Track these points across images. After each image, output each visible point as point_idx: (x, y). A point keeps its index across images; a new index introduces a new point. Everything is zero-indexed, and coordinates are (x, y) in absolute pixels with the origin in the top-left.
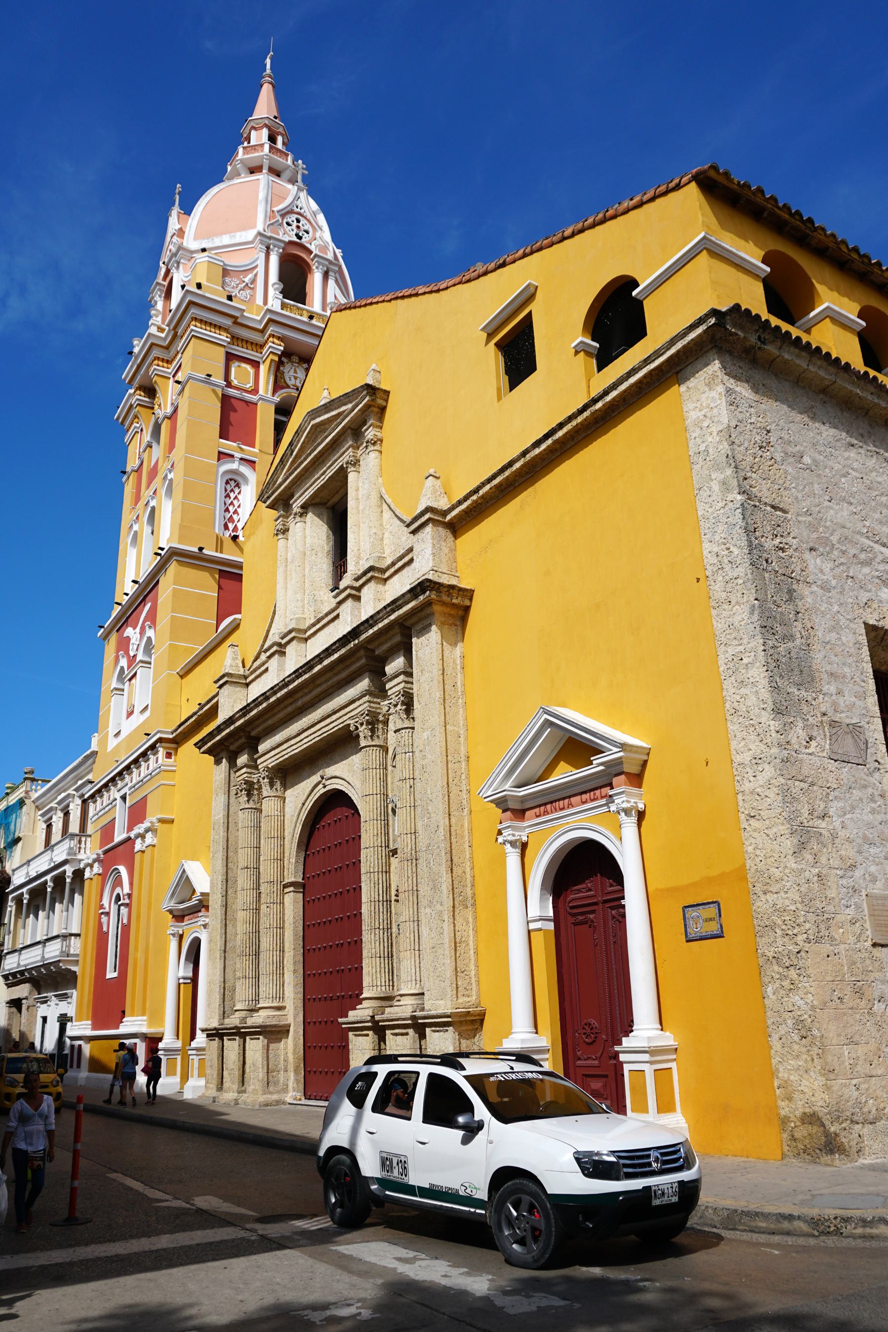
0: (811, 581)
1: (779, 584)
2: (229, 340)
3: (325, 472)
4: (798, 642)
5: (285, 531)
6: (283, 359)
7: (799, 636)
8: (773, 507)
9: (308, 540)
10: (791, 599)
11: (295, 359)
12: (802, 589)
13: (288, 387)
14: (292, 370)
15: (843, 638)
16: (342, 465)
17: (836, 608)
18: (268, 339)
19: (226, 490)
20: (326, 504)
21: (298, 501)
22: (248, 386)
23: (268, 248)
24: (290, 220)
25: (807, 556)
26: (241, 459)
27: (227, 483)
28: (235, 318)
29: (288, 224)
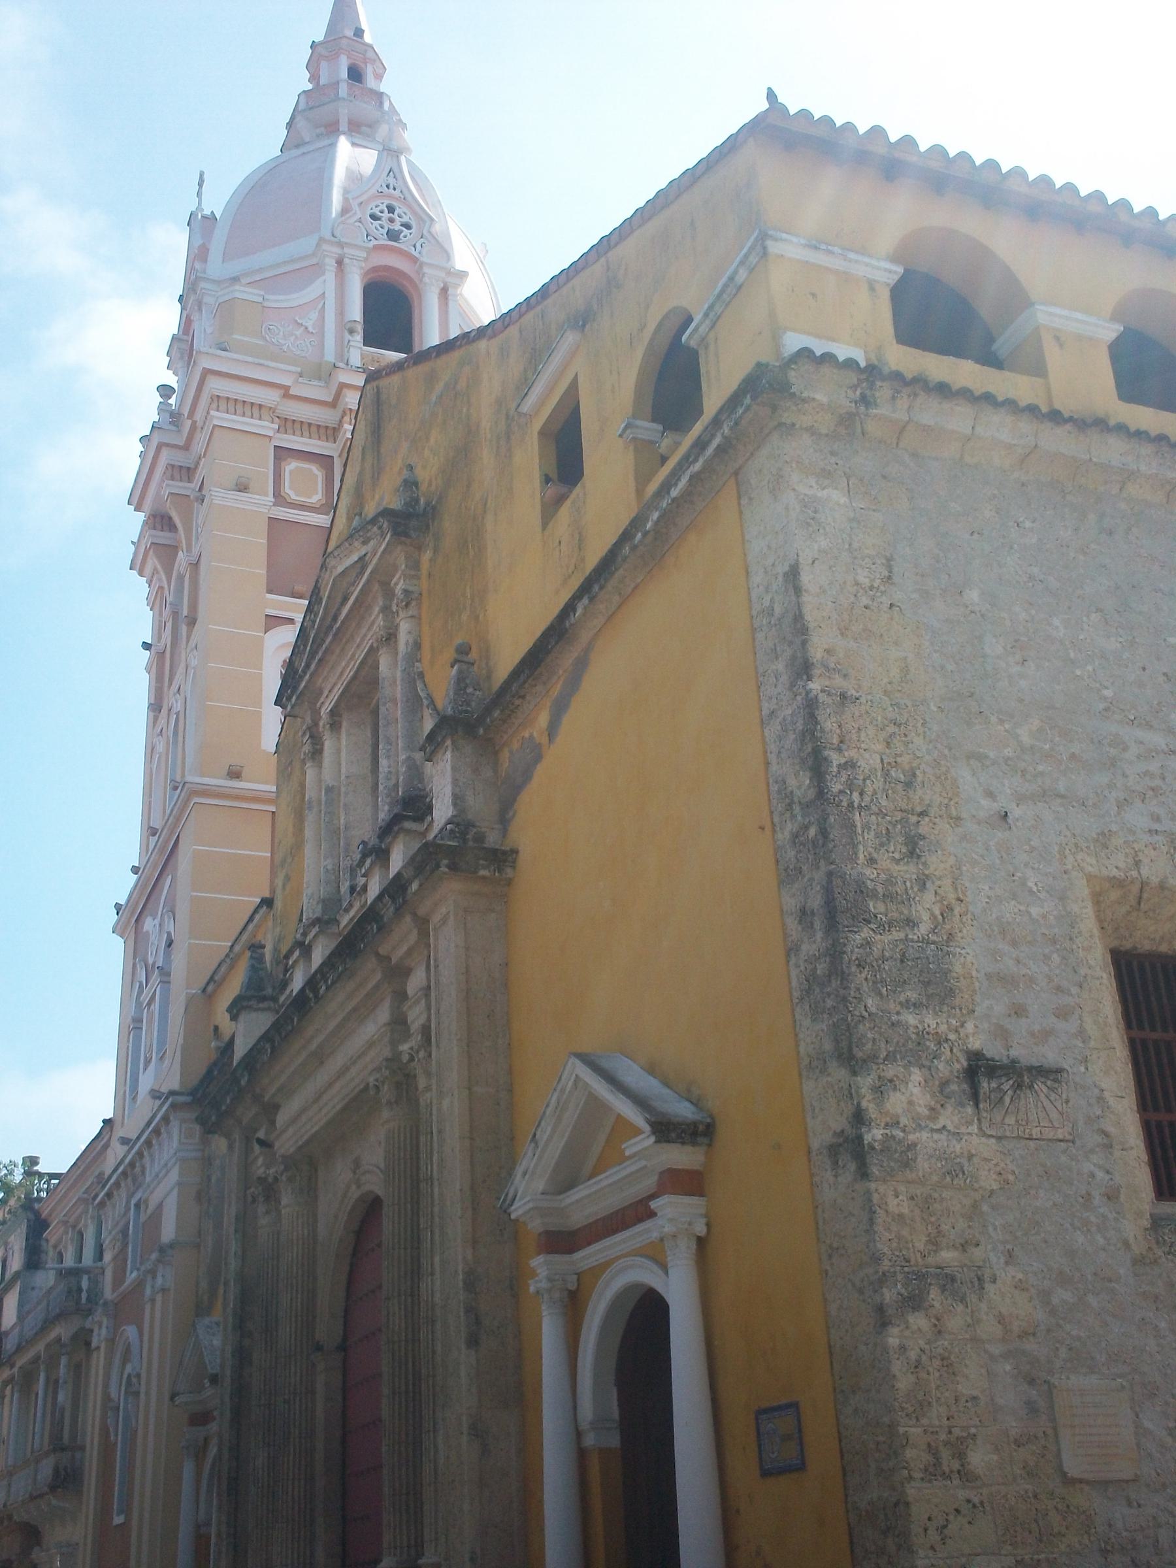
3: (353, 655)
16: (372, 646)
21: (327, 704)
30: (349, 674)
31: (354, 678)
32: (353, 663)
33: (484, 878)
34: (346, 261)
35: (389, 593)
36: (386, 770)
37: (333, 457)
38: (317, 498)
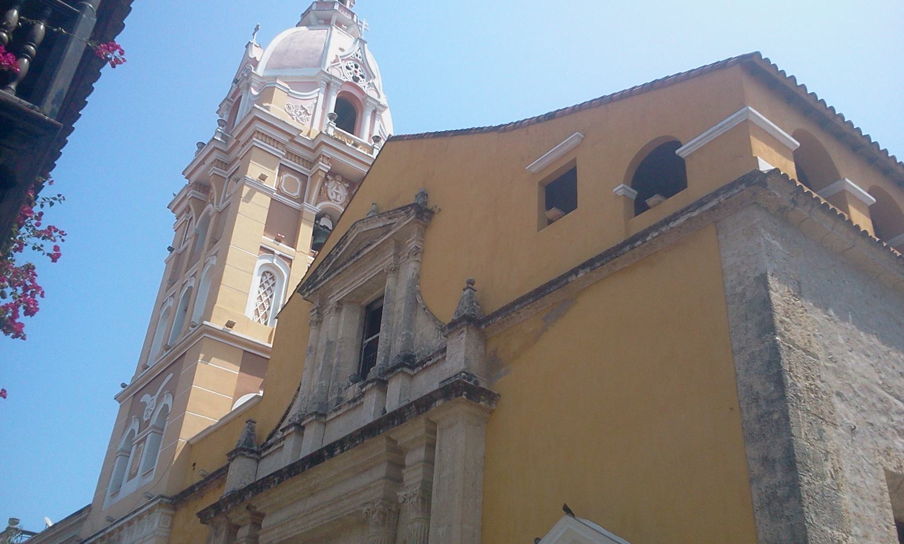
0: (838, 424)
1: (811, 423)
2: (284, 154)
4: (829, 481)
5: (319, 322)
6: (328, 176)
7: (829, 475)
8: (804, 350)
9: (341, 331)
10: (821, 439)
11: (339, 178)
12: (829, 430)
13: (329, 200)
14: (335, 187)
15: (868, 482)
16: (383, 271)
17: (860, 452)
18: (318, 158)
19: (262, 281)
20: (361, 302)
21: (335, 298)
22: (295, 195)
23: (328, 84)
24: (350, 66)
25: (835, 400)
26: (280, 255)
27: (264, 274)
28: (293, 137)
29: (347, 68)
30: (359, 283)
31: (361, 286)
32: (363, 278)
33: (480, 406)
34: (332, 84)
35: (399, 246)
36: (385, 338)
37: (307, 176)
38: (296, 194)
